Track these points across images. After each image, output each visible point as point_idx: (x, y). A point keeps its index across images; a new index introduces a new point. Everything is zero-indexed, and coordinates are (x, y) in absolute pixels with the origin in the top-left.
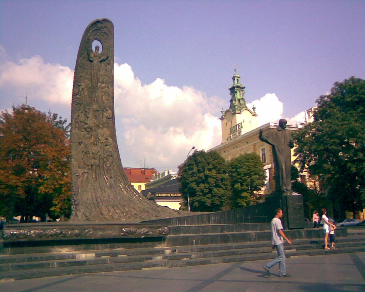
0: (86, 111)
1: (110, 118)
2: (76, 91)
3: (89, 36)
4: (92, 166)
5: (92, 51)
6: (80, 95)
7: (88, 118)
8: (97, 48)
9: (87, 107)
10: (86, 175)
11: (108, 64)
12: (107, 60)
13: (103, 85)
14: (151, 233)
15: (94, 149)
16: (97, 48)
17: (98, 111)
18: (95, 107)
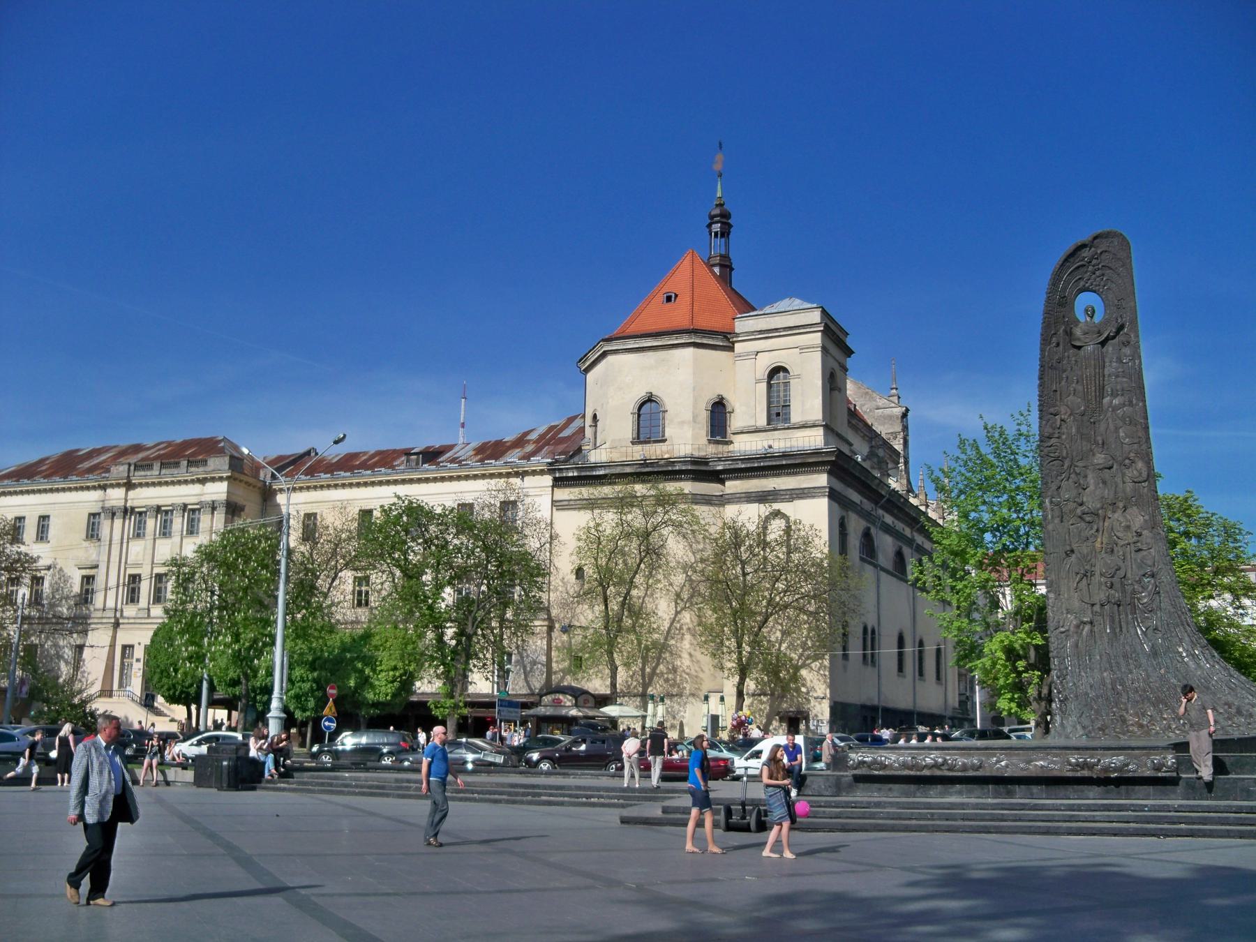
0: (1077, 474)
2: (1048, 430)
3: (1064, 289)
4: (1102, 605)
5: (1077, 322)
8: (1091, 312)
9: (1080, 464)
10: (1087, 628)
11: (1126, 344)
12: (1118, 333)
13: (1116, 402)
16: (1091, 312)
17: (1110, 468)
18: (1100, 459)
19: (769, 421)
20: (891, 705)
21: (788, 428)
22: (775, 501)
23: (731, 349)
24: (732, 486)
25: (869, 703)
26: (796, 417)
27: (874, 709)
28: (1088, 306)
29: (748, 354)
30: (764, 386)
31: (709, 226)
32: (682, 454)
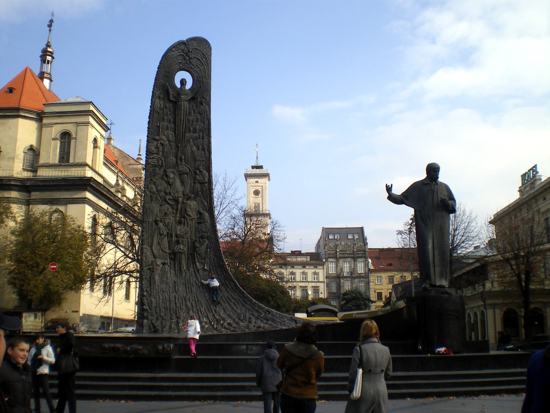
1: (206, 183)
6: (156, 154)
7: (170, 185)
8: (183, 82)
13: (195, 135)
14: (146, 352)
15: (180, 229)
16: (183, 82)
17: (187, 174)
19: (60, 161)
20: (120, 317)
21: (68, 165)
22: (57, 204)
24: (35, 195)
25: (106, 315)
26: (71, 161)
27: (109, 318)
28: (183, 78)
31: (41, 57)
32: (8, 175)
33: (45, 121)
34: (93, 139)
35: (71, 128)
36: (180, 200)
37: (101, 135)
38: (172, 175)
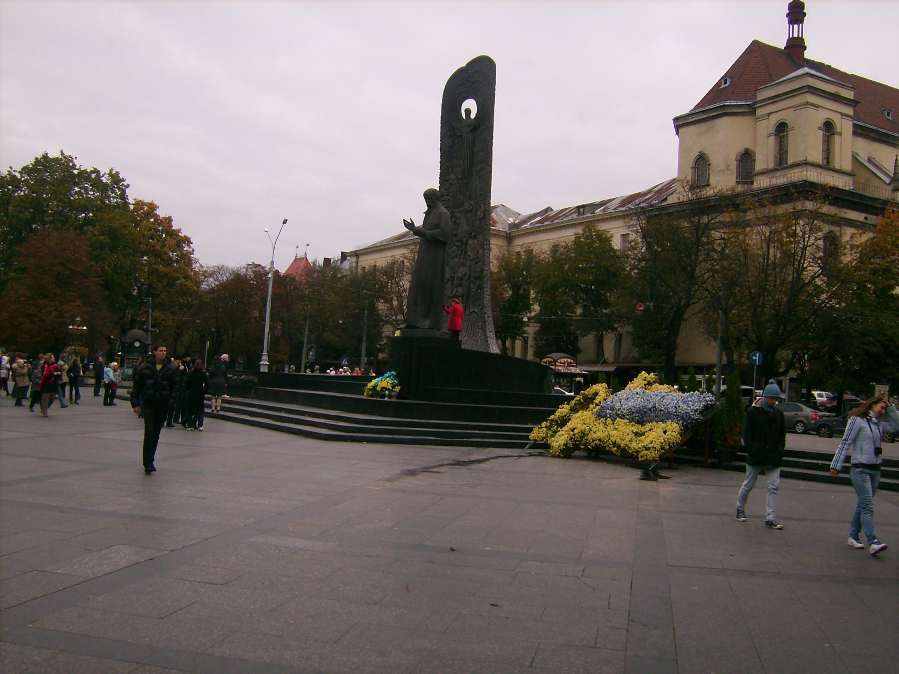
6: (448, 195)
8: (468, 112)
17: (470, 211)
18: (467, 206)
21: (785, 168)
23: (753, 112)
26: (791, 161)
29: (763, 116)
30: (772, 138)
33: (759, 112)
34: (820, 123)
35: (787, 116)
36: (465, 240)
37: (842, 114)
38: (459, 215)
